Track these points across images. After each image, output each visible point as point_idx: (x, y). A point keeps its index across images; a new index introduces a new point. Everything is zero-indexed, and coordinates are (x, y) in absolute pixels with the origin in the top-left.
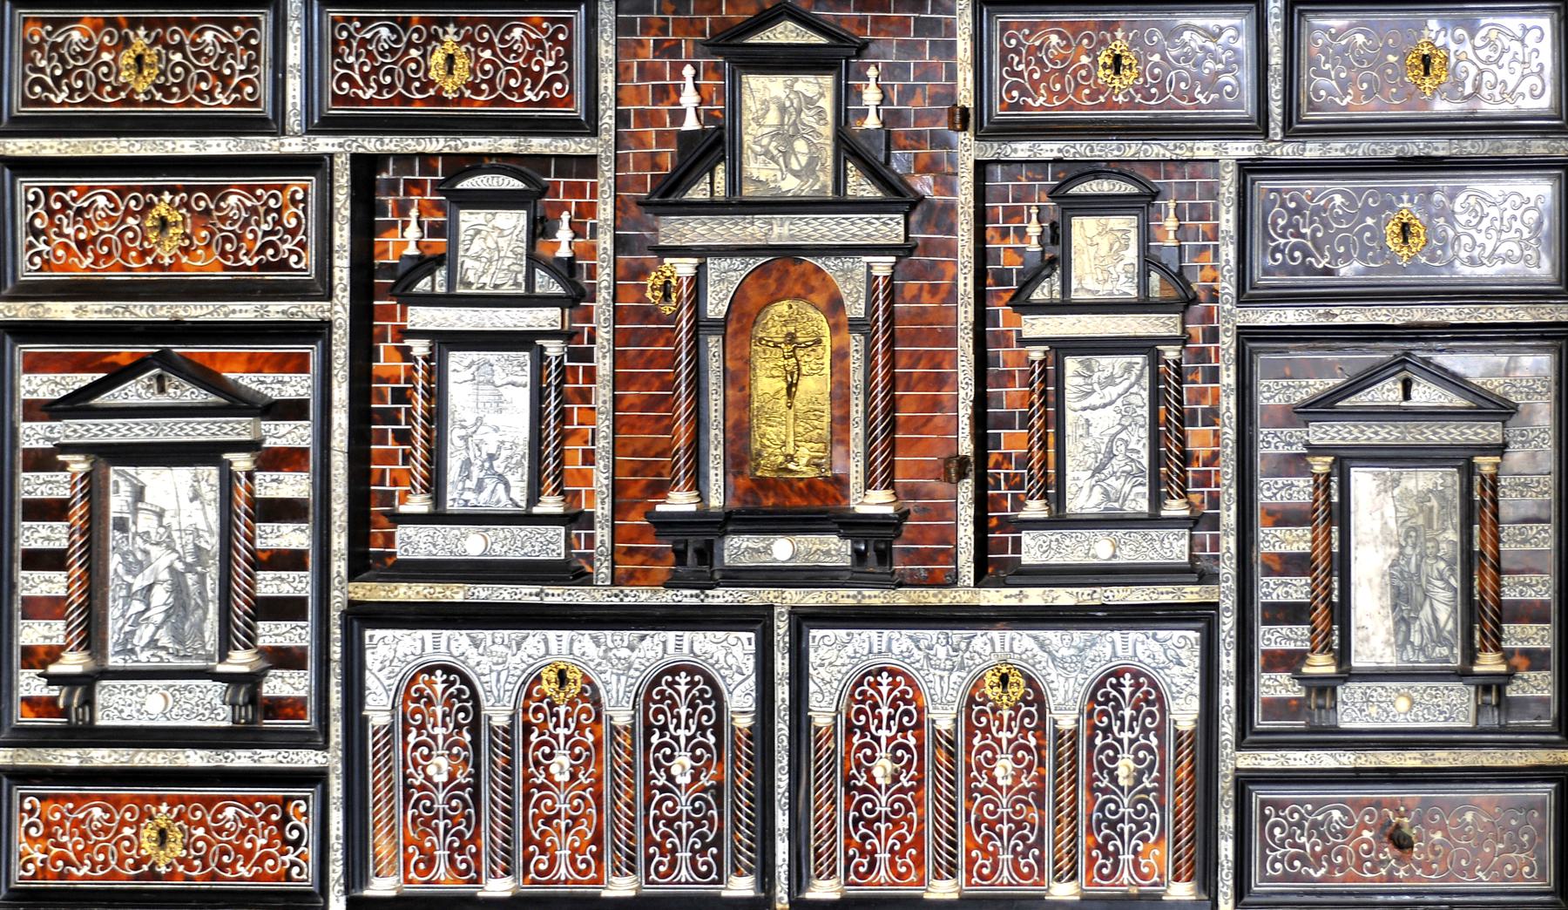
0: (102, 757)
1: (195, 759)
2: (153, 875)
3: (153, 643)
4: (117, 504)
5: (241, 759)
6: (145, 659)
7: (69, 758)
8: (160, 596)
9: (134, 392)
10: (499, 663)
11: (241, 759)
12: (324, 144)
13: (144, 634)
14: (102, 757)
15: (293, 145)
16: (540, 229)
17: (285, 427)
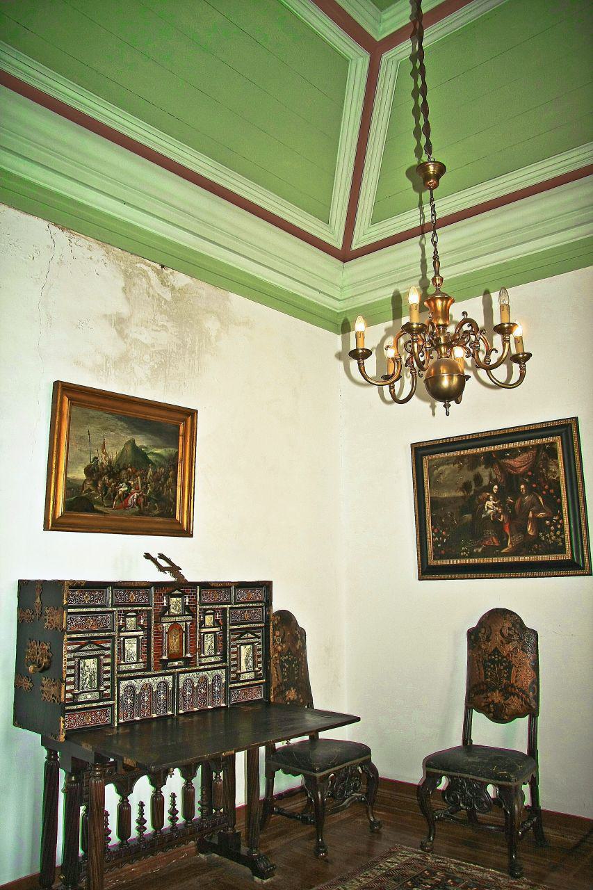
0: (80, 706)
1: (94, 705)
2: (86, 725)
3: (87, 687)
4: (81, 666)
5: (101, 704)
6: (86, 690)
7: (75, 707)
8: (88, 680)
9: (86, 648)
10: (138, 683)
11: (101, 704)
12: (115, 609)
13: (86, 685)
14: (80, 706)
15: (110, 609)
16: (138, 620)
17: (107, 652)
